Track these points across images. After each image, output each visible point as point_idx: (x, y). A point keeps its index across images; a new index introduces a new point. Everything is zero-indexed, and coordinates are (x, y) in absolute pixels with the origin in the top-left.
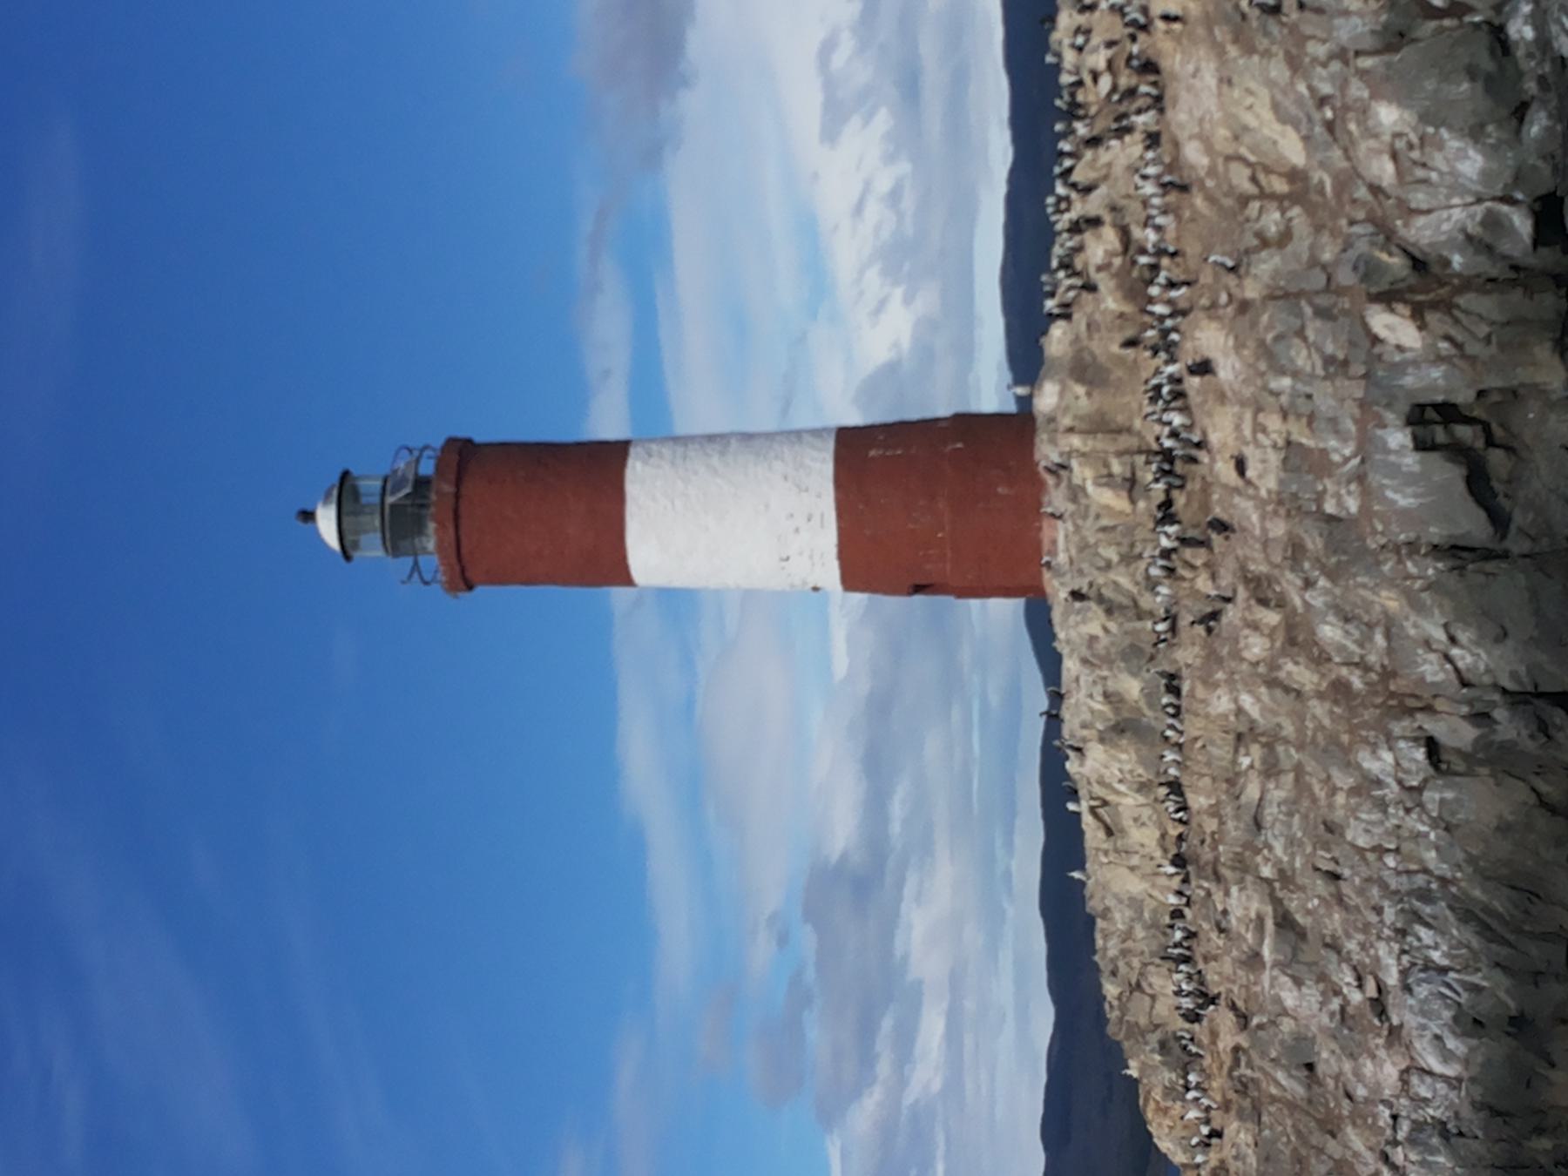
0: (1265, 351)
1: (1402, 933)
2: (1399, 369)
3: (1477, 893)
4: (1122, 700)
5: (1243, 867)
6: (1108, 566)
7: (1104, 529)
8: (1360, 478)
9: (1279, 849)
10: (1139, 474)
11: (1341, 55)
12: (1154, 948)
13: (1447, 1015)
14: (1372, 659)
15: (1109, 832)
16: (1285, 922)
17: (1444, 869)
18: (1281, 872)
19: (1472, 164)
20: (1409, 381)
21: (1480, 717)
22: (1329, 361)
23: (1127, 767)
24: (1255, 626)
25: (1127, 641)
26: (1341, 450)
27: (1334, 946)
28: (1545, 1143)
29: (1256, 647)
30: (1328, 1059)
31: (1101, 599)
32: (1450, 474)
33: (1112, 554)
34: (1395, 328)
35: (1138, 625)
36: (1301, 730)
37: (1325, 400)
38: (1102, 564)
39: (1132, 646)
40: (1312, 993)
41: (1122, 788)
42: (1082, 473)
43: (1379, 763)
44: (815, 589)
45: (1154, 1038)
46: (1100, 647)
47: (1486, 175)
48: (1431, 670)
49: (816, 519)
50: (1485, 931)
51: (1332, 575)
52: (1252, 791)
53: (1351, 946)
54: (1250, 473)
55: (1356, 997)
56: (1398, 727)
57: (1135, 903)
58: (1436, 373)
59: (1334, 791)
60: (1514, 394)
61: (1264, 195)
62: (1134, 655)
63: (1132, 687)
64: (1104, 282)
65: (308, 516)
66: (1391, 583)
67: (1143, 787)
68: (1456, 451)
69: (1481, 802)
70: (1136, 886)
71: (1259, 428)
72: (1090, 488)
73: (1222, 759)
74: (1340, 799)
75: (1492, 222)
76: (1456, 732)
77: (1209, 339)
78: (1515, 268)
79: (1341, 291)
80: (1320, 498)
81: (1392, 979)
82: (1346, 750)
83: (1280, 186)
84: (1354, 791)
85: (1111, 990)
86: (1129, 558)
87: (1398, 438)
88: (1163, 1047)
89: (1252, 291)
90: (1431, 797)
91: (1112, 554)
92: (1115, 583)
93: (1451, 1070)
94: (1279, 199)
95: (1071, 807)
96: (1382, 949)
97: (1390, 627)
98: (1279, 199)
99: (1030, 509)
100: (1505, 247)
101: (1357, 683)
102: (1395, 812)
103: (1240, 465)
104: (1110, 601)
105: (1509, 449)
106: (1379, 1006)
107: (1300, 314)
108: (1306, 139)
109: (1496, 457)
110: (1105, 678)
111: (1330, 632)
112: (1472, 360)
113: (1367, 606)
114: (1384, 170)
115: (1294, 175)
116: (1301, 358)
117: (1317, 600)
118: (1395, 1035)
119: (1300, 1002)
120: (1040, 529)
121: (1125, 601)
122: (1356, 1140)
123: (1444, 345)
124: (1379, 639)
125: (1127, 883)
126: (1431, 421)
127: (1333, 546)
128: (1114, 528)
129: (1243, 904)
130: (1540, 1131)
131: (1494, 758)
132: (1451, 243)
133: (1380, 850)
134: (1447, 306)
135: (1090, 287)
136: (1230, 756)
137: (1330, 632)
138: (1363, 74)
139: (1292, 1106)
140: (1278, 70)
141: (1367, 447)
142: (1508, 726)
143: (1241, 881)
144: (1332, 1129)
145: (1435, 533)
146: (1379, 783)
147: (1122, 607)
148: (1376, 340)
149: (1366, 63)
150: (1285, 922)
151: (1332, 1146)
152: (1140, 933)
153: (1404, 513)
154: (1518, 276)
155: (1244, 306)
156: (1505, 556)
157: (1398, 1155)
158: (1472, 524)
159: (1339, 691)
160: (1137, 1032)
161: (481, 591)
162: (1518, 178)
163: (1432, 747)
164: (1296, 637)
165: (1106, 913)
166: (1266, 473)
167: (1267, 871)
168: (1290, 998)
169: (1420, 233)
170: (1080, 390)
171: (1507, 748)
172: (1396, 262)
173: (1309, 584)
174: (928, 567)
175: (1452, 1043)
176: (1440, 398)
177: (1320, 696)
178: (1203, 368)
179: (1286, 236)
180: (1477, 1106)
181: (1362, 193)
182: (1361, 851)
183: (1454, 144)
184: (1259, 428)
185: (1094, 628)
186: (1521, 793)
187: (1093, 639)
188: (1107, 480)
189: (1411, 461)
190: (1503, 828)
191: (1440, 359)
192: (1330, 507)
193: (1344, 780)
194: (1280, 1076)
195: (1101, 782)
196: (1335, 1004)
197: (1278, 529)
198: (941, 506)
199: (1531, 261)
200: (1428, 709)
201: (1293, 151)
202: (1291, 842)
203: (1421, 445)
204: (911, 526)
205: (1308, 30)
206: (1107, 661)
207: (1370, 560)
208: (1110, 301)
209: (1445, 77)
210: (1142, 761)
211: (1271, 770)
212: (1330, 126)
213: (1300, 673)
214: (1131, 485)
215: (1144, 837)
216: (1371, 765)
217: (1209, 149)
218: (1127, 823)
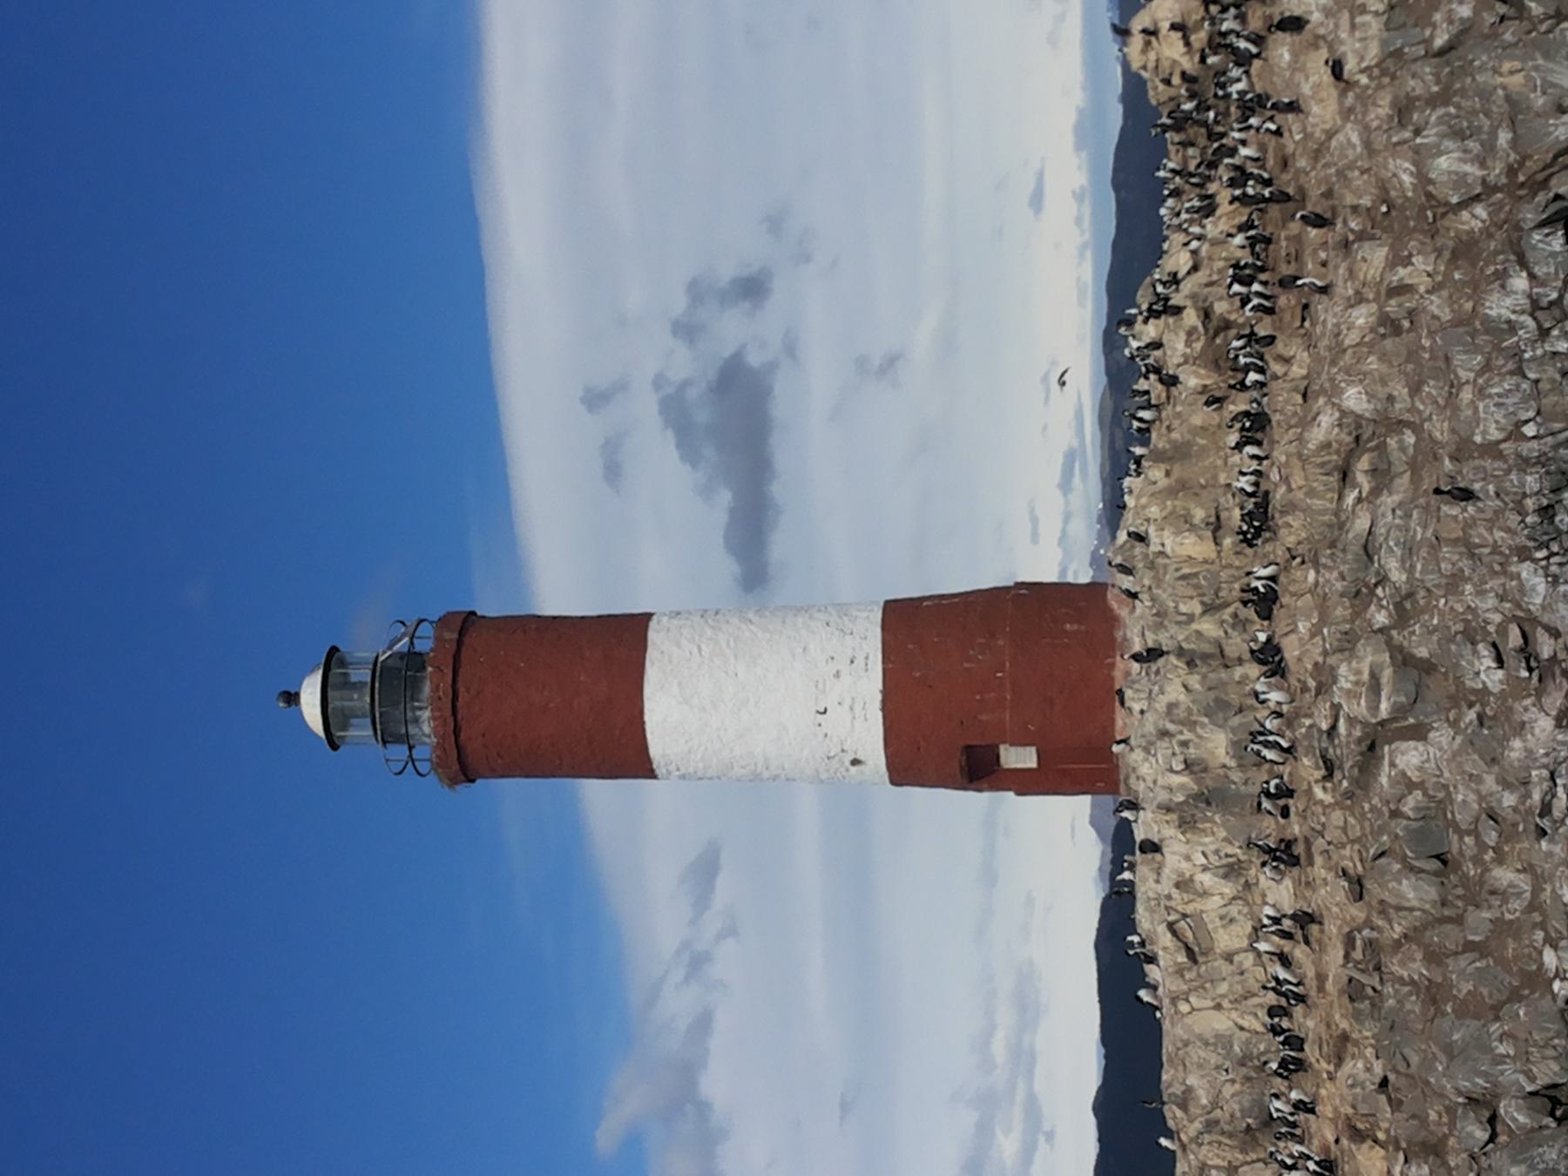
4: (1205, 770)
6: (1191, 618)
7: (1184, 577)
10: (1224, 515)
12: (1247, 1105)
23: (1212, 847)
25: (1212, 695)
31: (1181, 652)
35: (1223, 674)
38: (1183, 618)
39: (1217, 700)
44: (855, 762)
46: (1181, 713)
49: (860, 661)
62: (1218, 708)
65: (292, 698)
73: (1324, 512)
92: (1199, 633)
95: (1143, 994)
104: (1193, 651)
110: (1185, 744)
120: (1113, 665)
121: (1207, 648)
128: (1196, 575)
136: (1334, 505)
147: (1206, 657)
161: (479, 781)
174: (983, 717)
185: (1175, 692)
198: (1001, 642)
204: (966, 665)
206: (1192, 725)
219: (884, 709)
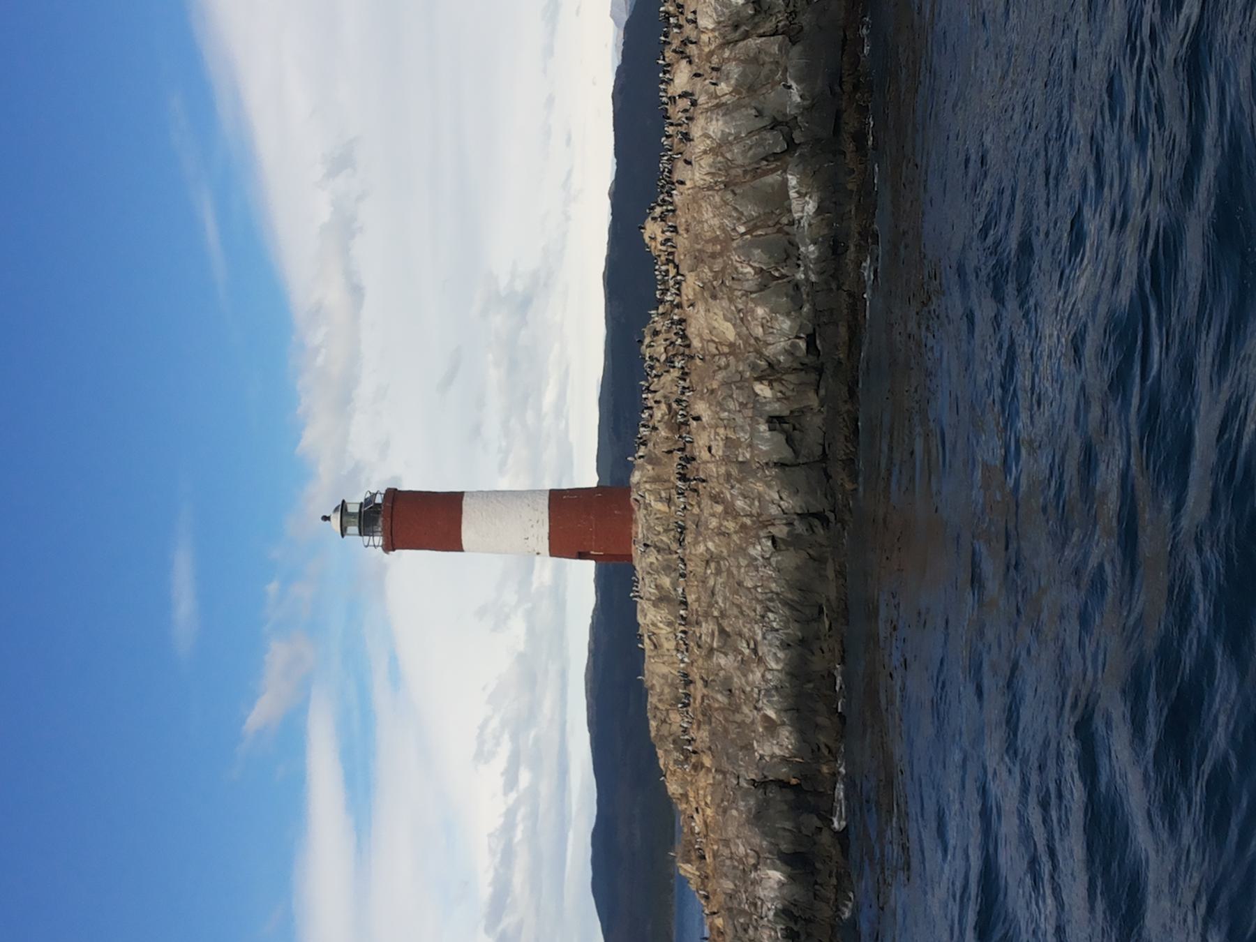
0: (720, 404)
1: (763, 617)
2: (765, 404)
3: (790, 596)
5: (707, 615)
8: (750, 445)
9: (720, 601)
11: (747, 293)
13: (778, 643)
14: (754, 512)
15: (655, 646)
16: (722, 631)
17: (778, 590)
18: (721, 612)
19: (785, 324)
20: (767, 408)
21: (790, 524)
22: (741, 404)
24: (713, 515)
26: (744, 437)
27: (740, 635)
28: (811, 685)
29: (714, 523)
30: (737, 681)
31: (656, 547)
32: (781, 438)
33: (660, 529)
34: (763, 390)
36: (729, 551)
37: (740, 421)
40: (731, 657)
41: (661, 625)
42: (650, 498)
43: (756, 551)
45: (670, 739)
47: (791, 327)
48: (774, 510)
50: (792, 608)
51: (739, 482)
52: (711, 582)
53: (745, 630)
54: (713, 451)
55: (747, 651)
56: (762, 534)
57: (664, 677)
58: (777, 405)
59: (739, 567)
60: (802, 411)
61: (720, 354)
62: (668, 569)
63: (666, 582)
64: (661, 426)
66: (760, 480)
67: (670, 624)
68: (783, 431)
69: (789, 559)
70: (665, 669)
71: (717, 434)
72: (653, 503)
74: (742, 570)
75: (794, 346)
76: (780, 531)
77: (701, 408)
78: (802, 364)
79: (746, 380)
80: (737, 456)
81: (759, 638)
82: (745, 550)
83: (726, 350)
84: (748, 566)
85: (653, 724)
86: (666, 531)
87: (763, 427)
88: (674, 742)
89: (715, 386)
90: (773, 560)
91: (660, 529)
93: (779, 667)
94: (725, 355)
96: (756, 627)
97: (760, 497)
98: (725, 355)
99: (629, 519)
100: (798, 354)
101: (748, 521)
102: (760, 569)
103: (710, 449)
105: (801, 431)
106: (755, 651)
107: (731, 389)
108: (734, 325)
109: (796, 432)
111: (740, 503)
112: (787, 398)
113: (753, 489)
114: (759, 331)
115: (731, 345)
116: (732, 407)
117: (735, 492)
118: (761, 660)
119: (725, 661)
122: (746, 710)
123: (779, 395)
124: (757, 503)
125: (659, 670)
126: (775, 421)
127: (740, 471)
129: (707, 628)
130: (809, 681)
131: (793, 541)
132: (780, 353)
133: (756, 587)
134: (780, 380)
135: (655, 428)
137: (740, 503)
138: (752, 300)
139: (722, 709)
140: (725, 303)
141: (754, 432)
142: (800, 527)
143: (707, 622)
144: (737, 710)
145: (775, 458)
146: (756, 559)
148: (757, 395)
149: (754, 296)
150: (722, 631)
151: (738, 718)
152: (667, 690)
153: (766, 452)
154: (804, 367)
155: (712, 391)
156: (799, 465)
157: (760, 705)
158: (786, 454)
159: (743, 527)
160: (662, 738)
162: (801, 327)
163: (774, 540)
164: (730, 512)
165: (653, 687)
166: (718, 451)
167: (716, 614)
168: (723, 661)
169: (769, 351)
170: (649, 467)
171: (799, 536)
172: (763, 363)
173: (732, 487)
175: (781, 655)
176: (777, 414)
177: (736, 532)
178: (697, 419)
179: (728, 365)
180: (788, 674)
181: (752, 341)
182: (748, 589)
183: (781, 318)
184: (717, 434)
185: (652, 559)
186: (804, 555)
187: (652, 563)
188: (661, 500)
189: (768, 434)
190: (798, 568)
191: (779, 400)
192: (740, 459)
193: (743, 562)
194: (719, 697)
195: (654, 624)
196: (739, 658)
197: (722, 470)
199: (806, 361)
200: (773, 524)
201: (730, 333)
202: (725, 598)
203: (770, 430)
205: (735, 287)
206: (658, 573)
207: (753, 473)
208: (663, 433)
209: (778, 296)
210: (670, 613)
211: (718, 572)
212: (742, 319)
213: (731, 525)
214: (669, 501)
215: (669, 645)
216: (752, 552)
217: (702, 339)
218: (663, 640)
219: (549, 538)
